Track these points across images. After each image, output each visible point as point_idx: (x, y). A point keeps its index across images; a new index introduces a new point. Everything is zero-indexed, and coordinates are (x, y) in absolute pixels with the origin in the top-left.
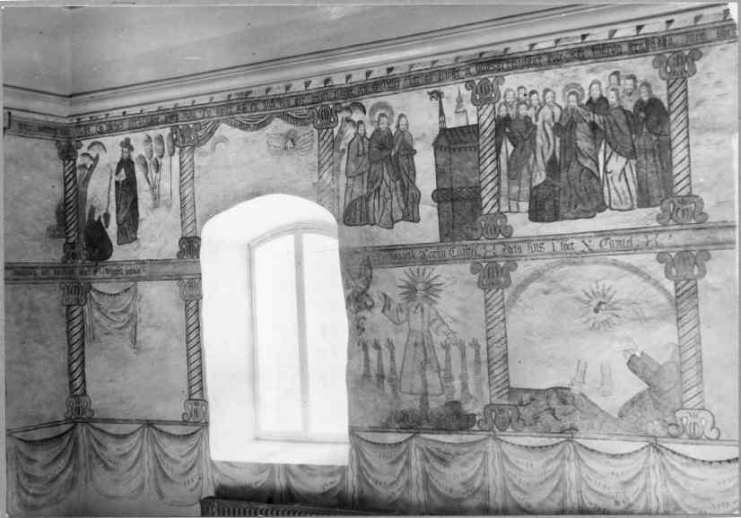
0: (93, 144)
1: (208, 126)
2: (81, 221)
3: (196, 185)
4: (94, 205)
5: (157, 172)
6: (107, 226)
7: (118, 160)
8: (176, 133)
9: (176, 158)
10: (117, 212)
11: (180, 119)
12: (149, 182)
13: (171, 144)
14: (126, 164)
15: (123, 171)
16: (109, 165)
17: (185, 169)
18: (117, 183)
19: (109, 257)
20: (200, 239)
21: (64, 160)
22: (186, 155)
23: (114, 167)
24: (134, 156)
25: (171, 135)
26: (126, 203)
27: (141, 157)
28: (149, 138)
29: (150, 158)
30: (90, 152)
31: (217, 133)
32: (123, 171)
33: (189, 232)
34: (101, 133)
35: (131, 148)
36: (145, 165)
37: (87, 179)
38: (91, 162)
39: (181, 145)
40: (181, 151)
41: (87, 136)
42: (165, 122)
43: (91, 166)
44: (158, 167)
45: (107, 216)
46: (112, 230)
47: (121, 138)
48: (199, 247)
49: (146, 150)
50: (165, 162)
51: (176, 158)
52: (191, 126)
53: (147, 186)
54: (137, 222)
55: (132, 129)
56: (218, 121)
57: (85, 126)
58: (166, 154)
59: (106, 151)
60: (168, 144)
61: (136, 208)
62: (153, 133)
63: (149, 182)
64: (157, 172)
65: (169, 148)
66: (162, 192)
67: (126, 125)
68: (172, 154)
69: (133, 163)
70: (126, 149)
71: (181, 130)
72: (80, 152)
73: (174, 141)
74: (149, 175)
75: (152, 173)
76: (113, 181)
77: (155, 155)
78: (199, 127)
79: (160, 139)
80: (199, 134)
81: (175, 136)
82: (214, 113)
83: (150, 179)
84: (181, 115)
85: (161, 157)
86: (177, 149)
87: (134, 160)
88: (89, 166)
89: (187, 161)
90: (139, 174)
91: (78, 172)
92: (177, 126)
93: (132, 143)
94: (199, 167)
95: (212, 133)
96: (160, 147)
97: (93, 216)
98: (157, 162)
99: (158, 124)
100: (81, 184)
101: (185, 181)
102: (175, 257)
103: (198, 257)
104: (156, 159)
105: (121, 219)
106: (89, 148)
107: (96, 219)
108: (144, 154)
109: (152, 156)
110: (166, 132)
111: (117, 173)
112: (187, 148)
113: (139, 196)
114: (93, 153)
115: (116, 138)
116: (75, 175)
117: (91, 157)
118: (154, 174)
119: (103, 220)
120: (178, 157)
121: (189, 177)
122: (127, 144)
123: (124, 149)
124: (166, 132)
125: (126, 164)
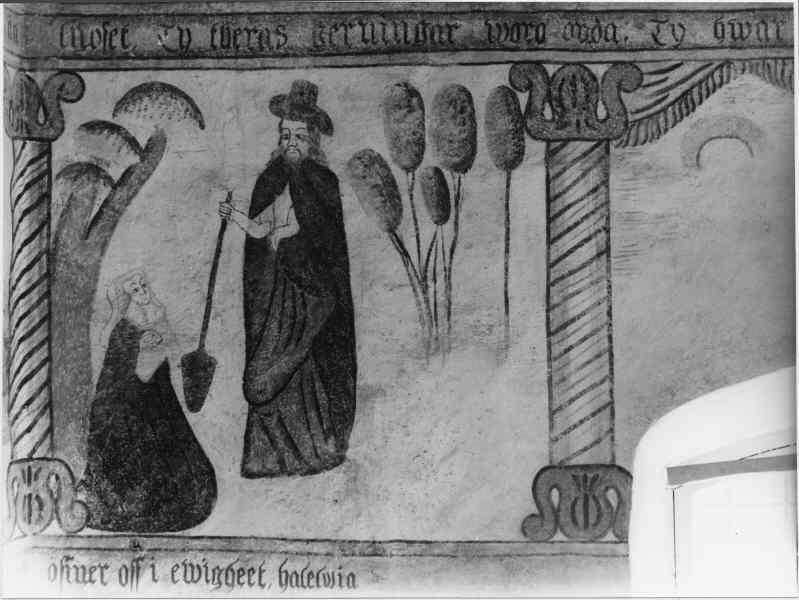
0: (145, 90)
1: (675, 76)
2: (63, 378)
3: (616, 280)
4: (135, 316)
5: (442, 219)
6: (195, 406)
7: (260, 160)
8: (530, 87)
9: (530, 181)
10: (251, 355)
11: (551, 41)
12: (405, 254)
13: (504, 123)
14: (302, 180)
15: (284, 204)
16: (212, 177)
17: (568, 218)
18: (254, 249)
19: (201, 519)
20: (627, 475)
21: (14, 139)
22: (573, 173)
23: (244, 192)
24: (337, 153)
25: (507, 94)
26: (297, 327)
27: (371, 160)
28: (413, 93)
29: (409, 170)
30: (124, 120)
31: (712, 108)
32: (284, 204)
33: (580, 446)
34: (185, 54)
35: (323, 124)
36: (389, 193)
37: (105, 220)
38: (133, 159)
39: (551, 131)
40: (550, 155)
41: (111, 60)
42: (486, 45)
43: (129, 172)
44: (444, 204)
45: (199, 368)
46: (218, 423)
47: (279, 80)
48: (624, 502)
49: (395, 140)
50: (479, 185)
51: (530, 181)
52: (599, 71)
53: (394, 267)
54: (351, 396)
55: (318, 52)
56: (728, 62)
57: (106, 19)
58: (484, 156)
59: (202, 127)
60: (490, 124)
61: (348, 345)
62: (428, 78)
63: (405, 254)
64: (442, 219)
65: (497, 141)
66: (460, 298)
67: (300, 35)
68: (511, 162)
69: (331, 179)
70: (295, 126)
71: (549, 81)
72: (74, 115)
73: (521, 123)
74: (406, 231)
75: (421, 226)
76: (235, 239)
77: (431, 159)
78: (630, 76)
79: (460, 103)
80: (635, 101)
81: (523, 98)
82: (702, 33)
83: (410, 246)
84: (555, 30)
85: (464, 166)
86: (535, 149)
87: (332, 167)
88: (115, 173)
89: (579, 191)
90: (360, 219)
91: (59, 191)
92: (539, 63)
93: (327, 103)
94: (630, 218)
95: (687, 103)
96: (455, 130)
97: (133, 351)
98: (442, 182)
99: (452, 48)
100: (70, 238)
101: (574, 261)
102: (514, 534)
103: (622, 538)
104: (437, 171)
105: (264, 380)
106: (122, 104)
107: (145, 370)
108: (383, 150)
109: (419, 157)
110: (486, 81)
111: (255, 210)
112: (578, 148)
113: (361, 305)
114: (140, 123)
115: (251, 77)
116: (46, 197)
117: (132, 142)
118: (428, 229)
119: (177, 380)
120: (540, 173)
121: (588, 251)
122: (302, 105)
123: (287, 123)
124: (486, 81)
125: (302, 180)
